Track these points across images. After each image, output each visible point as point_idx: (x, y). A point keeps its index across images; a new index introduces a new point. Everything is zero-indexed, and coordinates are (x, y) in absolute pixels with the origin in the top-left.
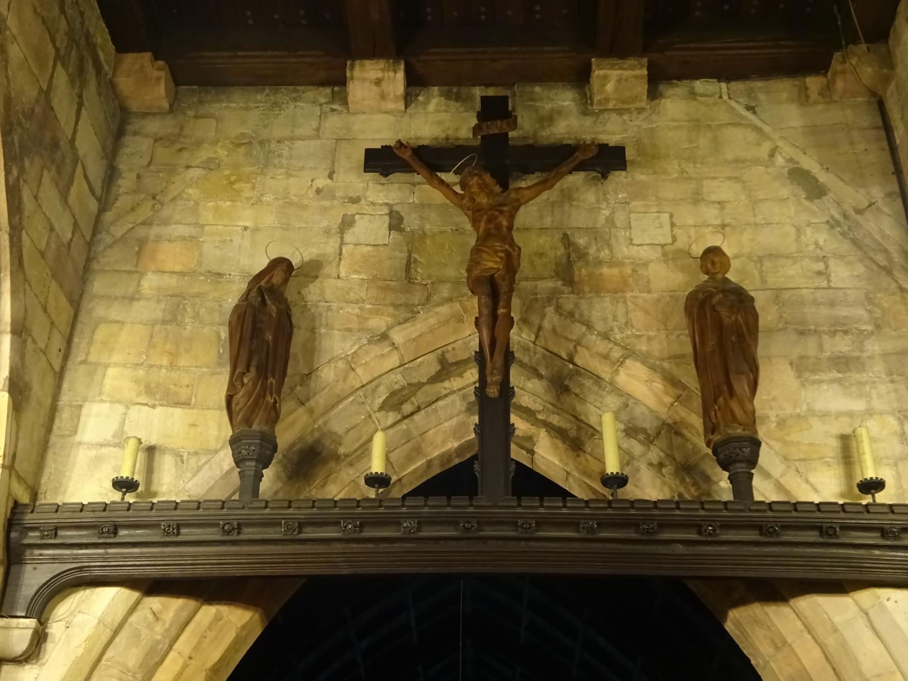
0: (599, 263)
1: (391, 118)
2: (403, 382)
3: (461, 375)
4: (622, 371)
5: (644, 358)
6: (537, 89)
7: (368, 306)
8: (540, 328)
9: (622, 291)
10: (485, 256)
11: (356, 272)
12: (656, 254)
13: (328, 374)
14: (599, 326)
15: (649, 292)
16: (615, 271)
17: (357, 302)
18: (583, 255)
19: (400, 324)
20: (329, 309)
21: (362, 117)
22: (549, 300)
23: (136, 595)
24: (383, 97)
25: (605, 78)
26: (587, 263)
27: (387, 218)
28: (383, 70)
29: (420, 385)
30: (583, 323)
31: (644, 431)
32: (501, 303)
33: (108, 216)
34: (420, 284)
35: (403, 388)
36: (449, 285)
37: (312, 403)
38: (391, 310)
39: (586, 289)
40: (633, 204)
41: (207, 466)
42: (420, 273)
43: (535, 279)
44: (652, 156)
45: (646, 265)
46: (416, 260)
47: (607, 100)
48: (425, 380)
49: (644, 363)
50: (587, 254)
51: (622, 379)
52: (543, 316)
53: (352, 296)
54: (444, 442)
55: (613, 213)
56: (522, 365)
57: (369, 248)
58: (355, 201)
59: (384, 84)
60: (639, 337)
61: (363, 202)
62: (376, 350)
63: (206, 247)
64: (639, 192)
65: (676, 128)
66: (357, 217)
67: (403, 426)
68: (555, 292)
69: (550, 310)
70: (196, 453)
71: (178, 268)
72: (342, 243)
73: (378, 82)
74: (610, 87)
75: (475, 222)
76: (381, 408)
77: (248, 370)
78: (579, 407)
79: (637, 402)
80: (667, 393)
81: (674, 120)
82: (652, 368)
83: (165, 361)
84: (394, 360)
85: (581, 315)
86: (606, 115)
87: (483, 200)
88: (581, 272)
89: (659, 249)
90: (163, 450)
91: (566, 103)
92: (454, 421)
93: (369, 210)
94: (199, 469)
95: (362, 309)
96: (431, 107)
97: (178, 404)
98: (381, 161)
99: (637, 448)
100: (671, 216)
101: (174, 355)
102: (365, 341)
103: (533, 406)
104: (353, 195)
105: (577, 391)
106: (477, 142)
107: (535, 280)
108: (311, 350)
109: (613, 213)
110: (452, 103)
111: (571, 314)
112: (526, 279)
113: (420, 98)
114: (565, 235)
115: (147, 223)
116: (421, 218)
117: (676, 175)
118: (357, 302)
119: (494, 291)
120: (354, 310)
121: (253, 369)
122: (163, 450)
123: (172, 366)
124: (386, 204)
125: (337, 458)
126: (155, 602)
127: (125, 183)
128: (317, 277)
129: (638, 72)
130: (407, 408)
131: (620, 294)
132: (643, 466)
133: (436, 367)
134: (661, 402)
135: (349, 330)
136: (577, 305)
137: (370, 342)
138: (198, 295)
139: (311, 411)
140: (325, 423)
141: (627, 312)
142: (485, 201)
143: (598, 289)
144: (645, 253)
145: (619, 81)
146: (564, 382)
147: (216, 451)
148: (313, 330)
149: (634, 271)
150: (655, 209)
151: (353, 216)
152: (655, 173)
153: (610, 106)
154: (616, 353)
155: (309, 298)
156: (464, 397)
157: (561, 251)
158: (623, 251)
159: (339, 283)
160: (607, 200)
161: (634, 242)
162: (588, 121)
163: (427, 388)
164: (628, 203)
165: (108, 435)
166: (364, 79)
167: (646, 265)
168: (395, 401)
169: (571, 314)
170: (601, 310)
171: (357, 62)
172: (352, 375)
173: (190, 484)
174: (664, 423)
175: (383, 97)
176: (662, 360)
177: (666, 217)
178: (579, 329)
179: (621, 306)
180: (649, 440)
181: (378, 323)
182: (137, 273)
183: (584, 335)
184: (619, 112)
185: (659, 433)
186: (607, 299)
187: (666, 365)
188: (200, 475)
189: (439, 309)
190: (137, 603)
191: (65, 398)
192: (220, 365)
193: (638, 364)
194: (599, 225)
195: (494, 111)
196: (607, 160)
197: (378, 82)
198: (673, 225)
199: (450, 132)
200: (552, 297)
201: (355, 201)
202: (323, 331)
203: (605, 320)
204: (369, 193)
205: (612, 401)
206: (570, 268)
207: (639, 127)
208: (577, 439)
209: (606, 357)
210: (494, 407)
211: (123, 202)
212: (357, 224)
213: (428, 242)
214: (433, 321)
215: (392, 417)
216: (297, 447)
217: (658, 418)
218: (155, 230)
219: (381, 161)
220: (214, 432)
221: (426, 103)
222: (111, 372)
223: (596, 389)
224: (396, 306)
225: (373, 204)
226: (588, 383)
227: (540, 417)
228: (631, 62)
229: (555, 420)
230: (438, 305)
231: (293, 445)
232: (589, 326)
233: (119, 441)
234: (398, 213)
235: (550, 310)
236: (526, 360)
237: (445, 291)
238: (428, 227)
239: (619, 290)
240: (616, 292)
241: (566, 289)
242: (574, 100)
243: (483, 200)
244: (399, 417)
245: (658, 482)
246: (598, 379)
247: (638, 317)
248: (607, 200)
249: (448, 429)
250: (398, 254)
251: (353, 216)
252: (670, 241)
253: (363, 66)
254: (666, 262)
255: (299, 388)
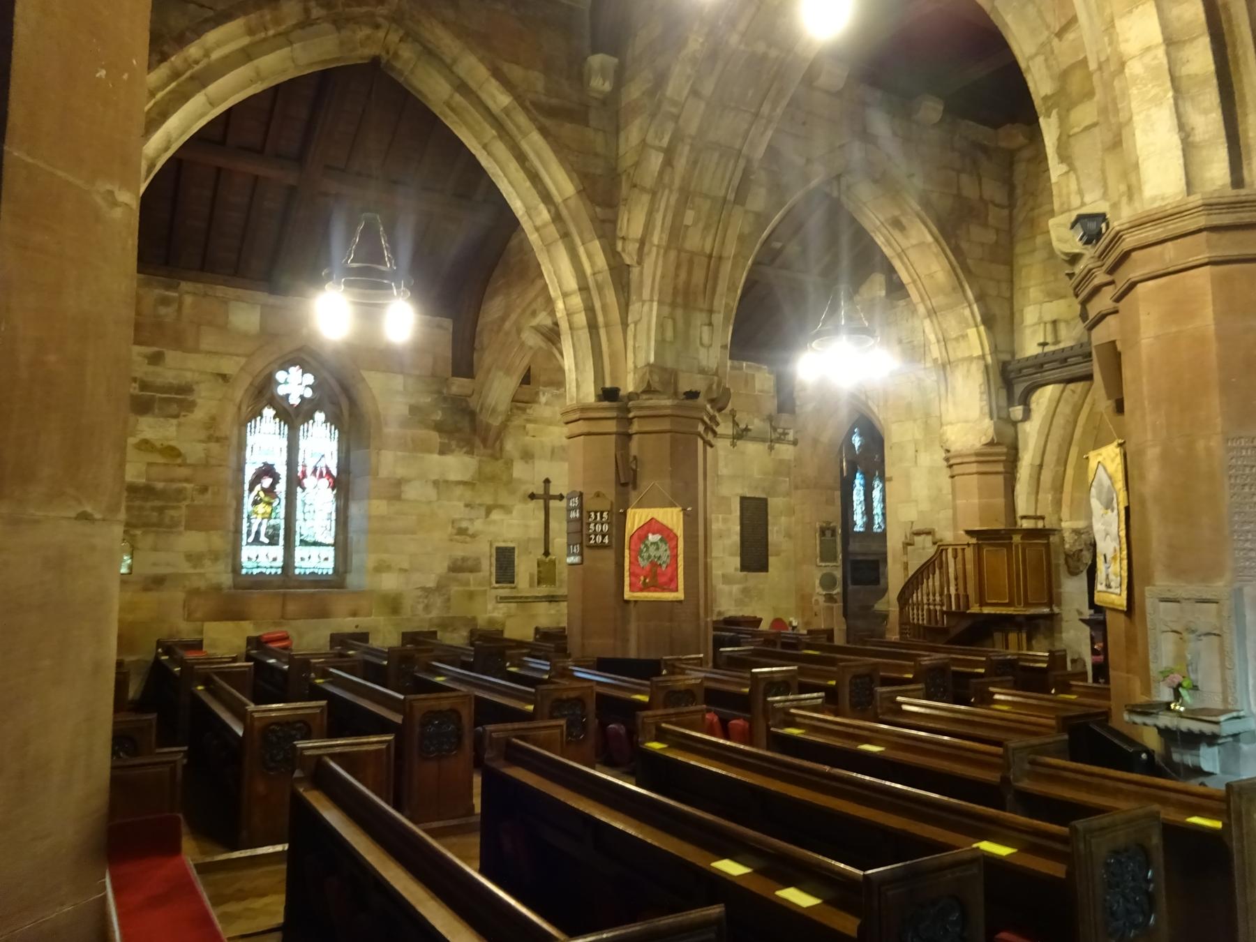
23: (1062, 386)
33: (1015, 211)
115: (1032, 209)
123: (1056, 280)
126: (1071, 386)
127: (1019, 191)
165: (1036, 320)
182: (1033, 237)
190: (1063, 391)
191: (1016, 308)
211: (1019, 203)
218: (1036, 211)
222: (1032, 290)
233: (1041, 321)
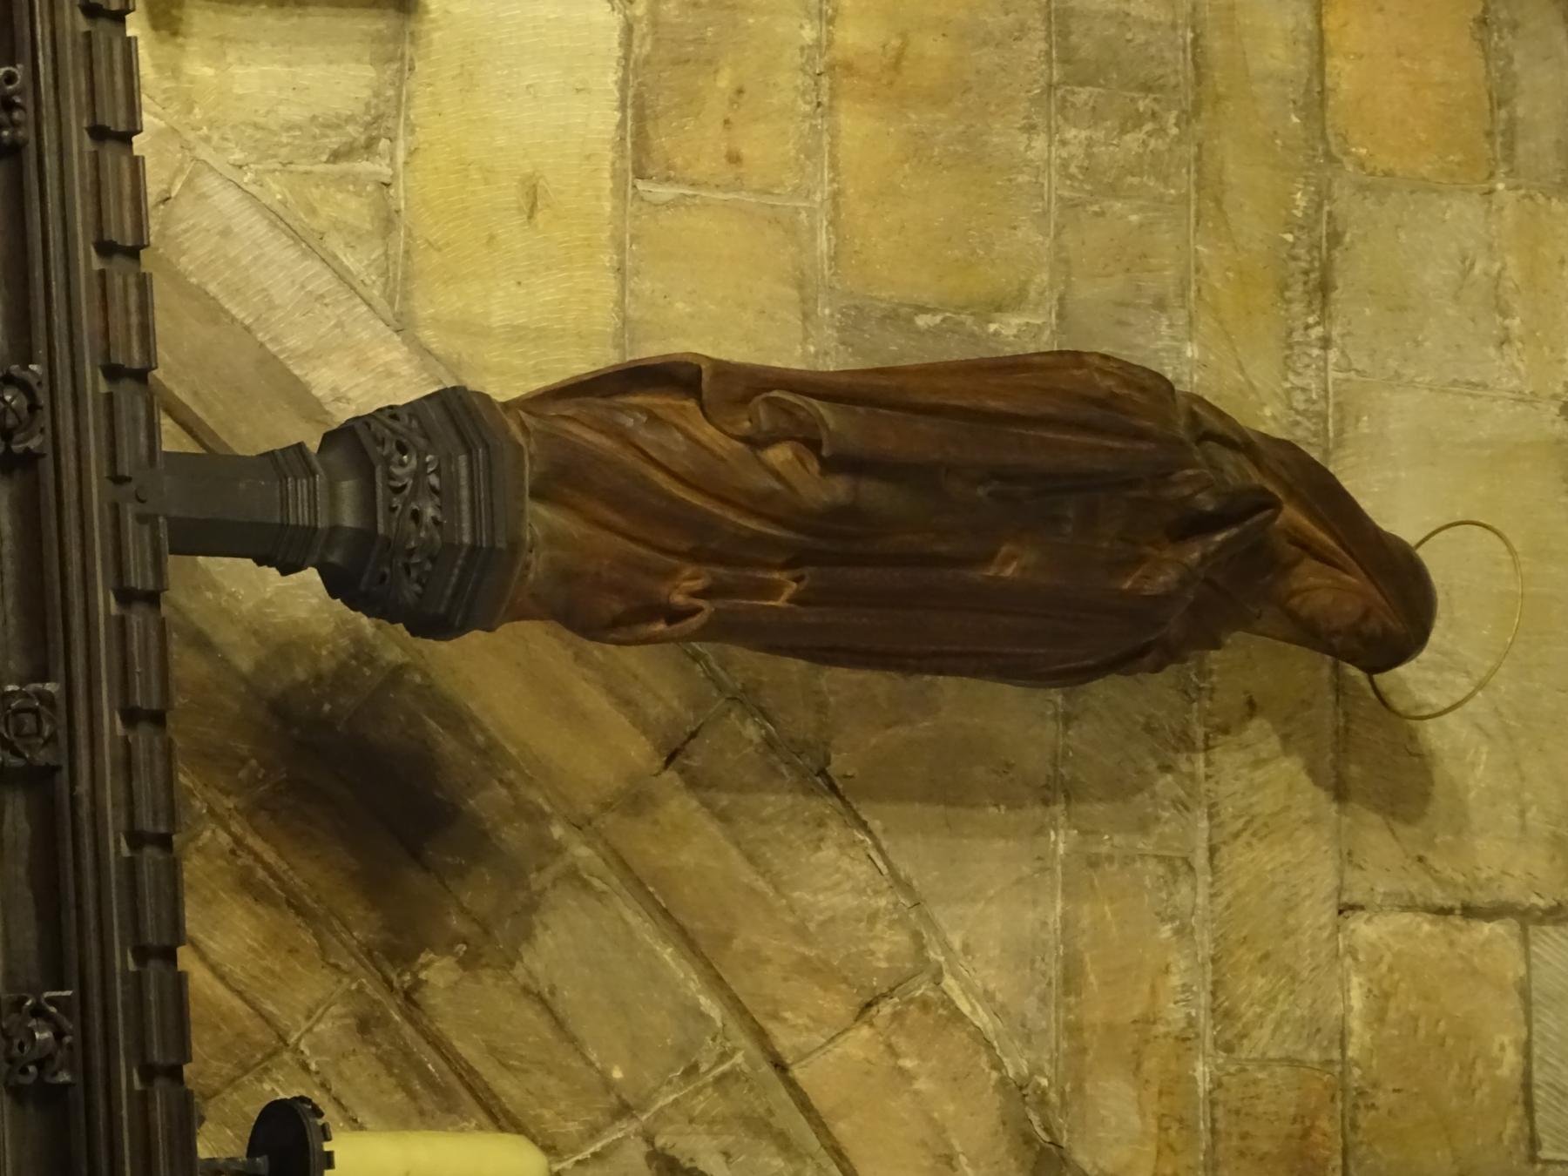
7: (1201, 1071)
11: (1380, 998)
13: (834, 879)
17: (1223, 1014)
20: (1178, 867)
37: (680, 805)
41: (324, 281)
53: (1252, 986)
57: (1511, 1059)
63: (1462, 211)
70: (388, 222)
71: (1343, 73)
72: (1525, 917)
77: (835, 465)
83: (853, 37)
90: (397, 56)
94: (307, 242)
95: (1185, 1040)
97: (639, 114)
101: (890, 82)
108: (952, 785)
118: (1223, 1014)
120: (1179, 999)
121: (839, 489)
122: (397, 56)
123: (833, 74)
125: (398, 948)
128: (1341, 793)
135: (1071, 979)
137: (1017, 1091)
138: (1210, 187)
139: (635, 801)
140: (575, 877)
147: (402, 325)
148: (1057, 789)
155: (1229, 759)
159: (1316, 915)
172: (837, 1005)
173: (227, 200)
188: (281, 251)
192: (854, 319)
202: (1061, 842)
216: (448, 744)
220: (502, 305)
231: (457, 720)
255: (751, 731)
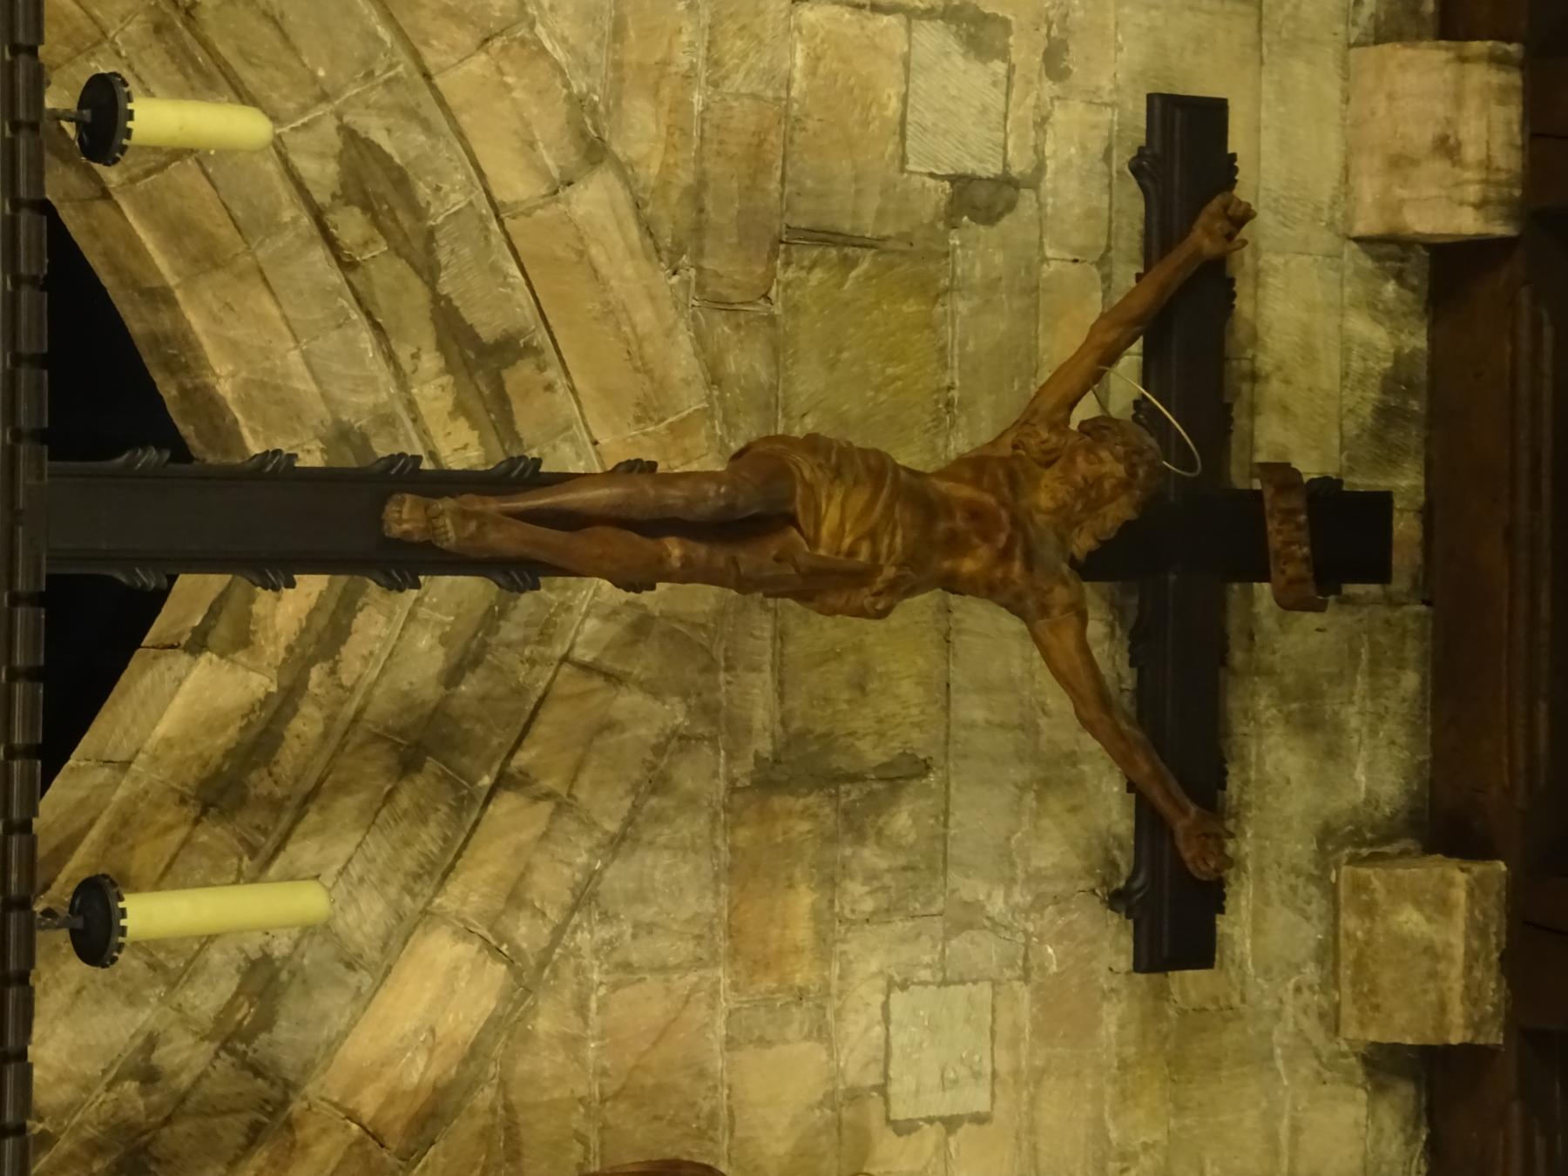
0: (830, 881)
1: (1326, 190)
2: (438, 215)
3: (460, 409)
4: (467, 950)
5: (507, 1024)
6: (1411, 680)
7: (697, 99)
8: (614, 679)
9: (734, 954)
10: (859, 499)
11: (815, 60)
12: (855, 1067)
14: (618, 877)
15: (730, 1043)
16: (802, 933)
17: (714, 63)
18: (856, 825)
19: (638, 206)
21: (1332, 90)
22: (709, 711)
24: (1399, 163)
25: (1442, 906)
26: (832, 840)
27: (992, 169)
28: (1487, 164)
29: (429, 271)
30: (630, 821)
31: (265, 1022)
32: (701, 551)
34: (770, 276)
35: (418, 212)
36: (764, 375)
38: (685, 177)
39: (743, 835)
40: (1024, 992)
42: (807, 278)
43: (779, 667)
44: (1181, 1057)
45: (821, 1033)
46: (848, 264)
47: (1369, 910)
48: (446, 286)
49: (494, 1023)
50: (860, 838)
51: (441, 950)
52: (653, 690)
54: (234, 349)
55: (995, 926)
56: (492, 619)
57: (894, 105)
58: (1054, 61)
59: (1440, 166)
60: (581, 1009)
61: (1049, 88)
62: (550, 125)
64: (1062, 1014)
65: (1272, 1138)
66: (999, 67)
67: (291, 211)
68: (733, 729)
69: (674, 712)
73: (1447, 148)
74: (1410, 920)
75: (975, 466)
76: (350, 135)
78: (347, 805)
79: (363, 1000)
80: (391, 1099)
81: (1295, 1129)
82: (475, 1052)
84: (515, 183)
85: (658, 818)
86: (1317, 907)
87: (1046, 494)
88: (800, 818)
89: (872, 1078)
91: (1361, 777)
92: (304, 385)
93: (1023, 111)
95: (688, 77)
96: (1360, 325)
98: (1185, 151)
99: (209, 996)
100: (980, 1119)
102: (579, 85)
103: (352, 654)
104: (1074, 59)
105: (404, 800)
106: (1239, 478)
107: (779, 665)
109: (995, 926)
110: (1373, 395)
111: (660, 783)
112: (781, 635)
113: (1390, 288)
114: (926, 767)
116: (992, 285)
117: (1114, 1135)
118: (714, 63)
119: (738, 525)
124: (1040, 168)
129: (1457, 1012)
130: (351, 226)
131: (723, 945)
132: (144, 1017)
133: (488, 325)
134: (362, 1077)
135: (618, 32)
136: (691, 802)
137: (578, 103)
141: (663, 968)
142: (1044, 500)
143: (743, 874)
144: (859, 1030)
145: (1429, 950)
146: (434, 758)
149: (801, 995)
150: (1004, 1062)
151: (1004, 54)
152: (1124, 1066)
153: (1349, 922)
154: (526, 932)
156: (386, 421)
157: (872, 754)
158: (869, 958)
160: (1038, 905)
161: (897, 997)
162: (1300, 849)
163: (418, 294)
164: (1026, 978)
166: (1458, 100)
167: (821, 1033)
168: (374, 182)
169: (660, 783)
170: (672, 883)
171: (1515, 78)
172: (466, 38)
174: (290, 1087)
175: (1399, 163)
176: (503, 1085)
177: (976, 1099)
178: (609, 807)
179: (686, 948)
180: (231, 1037)
181: (641, 134)
183: (589, 825)
184: (1328, 953)
185: (257, 1071)
186: (708, 905)
187: (486, 1096)
189: (684, 339)
193: (488, 1004)
194: (955, 878)
195: (1343, 536)
196: (1170, 910)
197: (1447, 148)
198: (951, 1123)
199: (1275, 387)
200: (718, 722)
201: (1054, 61)
203: (640, 897)
204: (1077, 107)
205: (366, 917)
206: (816, 781)
207: (1277, 1015)
208: (239, 800)
209: (516, 898)
210: (351, 520)
212: (976, 68)
213: (911, 307)
214: (644, 317)
215: (320, 172)
217: (307, 1068)
219: (1185, 151)
221: (1374, 308)
223: (409, 863)
224: (696, 193)
225: (1042, 123)
226: (429, 838)
227: (316, 674)
228: (1492, 989)
229: (306, 724)
230: (700, 339)
232: (617, 844)
234: (1011, 206)
235: (674, 712)
236: (510, 630)
237: (746, 361)
238: (962, 307)
239: (740, 945)
240: (732, 932)
241: (743, 770)
242: (1372, 800)
243: (1046, 494)
244: (321, 197)
245: (92, 1068)
246: (442, 870)
247: (646, 1005)
248: (1038, 905)
249: (280, 363)
250: (872, 204)
251: (1004, 54)
252: (900, 1112)
253: (1502, 95)
254: (829, 1100)
